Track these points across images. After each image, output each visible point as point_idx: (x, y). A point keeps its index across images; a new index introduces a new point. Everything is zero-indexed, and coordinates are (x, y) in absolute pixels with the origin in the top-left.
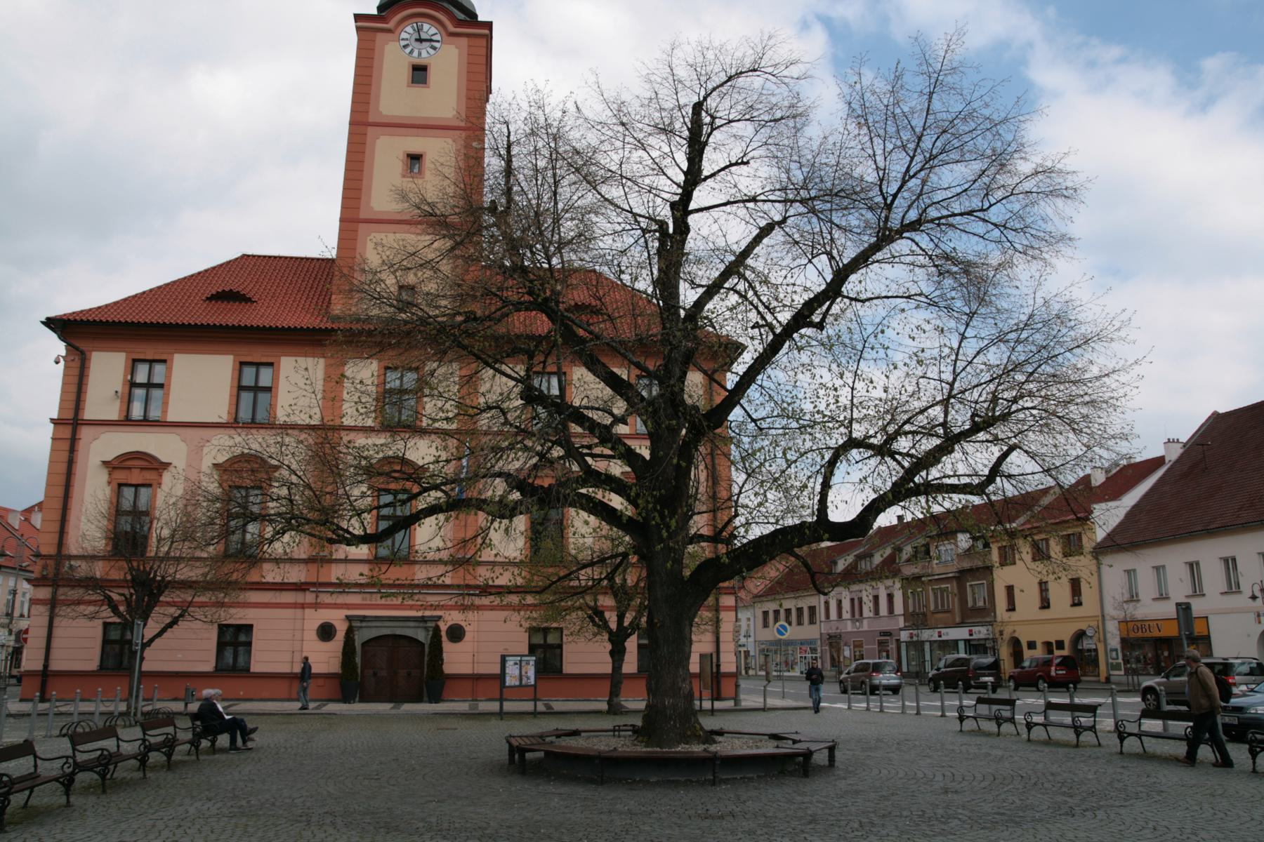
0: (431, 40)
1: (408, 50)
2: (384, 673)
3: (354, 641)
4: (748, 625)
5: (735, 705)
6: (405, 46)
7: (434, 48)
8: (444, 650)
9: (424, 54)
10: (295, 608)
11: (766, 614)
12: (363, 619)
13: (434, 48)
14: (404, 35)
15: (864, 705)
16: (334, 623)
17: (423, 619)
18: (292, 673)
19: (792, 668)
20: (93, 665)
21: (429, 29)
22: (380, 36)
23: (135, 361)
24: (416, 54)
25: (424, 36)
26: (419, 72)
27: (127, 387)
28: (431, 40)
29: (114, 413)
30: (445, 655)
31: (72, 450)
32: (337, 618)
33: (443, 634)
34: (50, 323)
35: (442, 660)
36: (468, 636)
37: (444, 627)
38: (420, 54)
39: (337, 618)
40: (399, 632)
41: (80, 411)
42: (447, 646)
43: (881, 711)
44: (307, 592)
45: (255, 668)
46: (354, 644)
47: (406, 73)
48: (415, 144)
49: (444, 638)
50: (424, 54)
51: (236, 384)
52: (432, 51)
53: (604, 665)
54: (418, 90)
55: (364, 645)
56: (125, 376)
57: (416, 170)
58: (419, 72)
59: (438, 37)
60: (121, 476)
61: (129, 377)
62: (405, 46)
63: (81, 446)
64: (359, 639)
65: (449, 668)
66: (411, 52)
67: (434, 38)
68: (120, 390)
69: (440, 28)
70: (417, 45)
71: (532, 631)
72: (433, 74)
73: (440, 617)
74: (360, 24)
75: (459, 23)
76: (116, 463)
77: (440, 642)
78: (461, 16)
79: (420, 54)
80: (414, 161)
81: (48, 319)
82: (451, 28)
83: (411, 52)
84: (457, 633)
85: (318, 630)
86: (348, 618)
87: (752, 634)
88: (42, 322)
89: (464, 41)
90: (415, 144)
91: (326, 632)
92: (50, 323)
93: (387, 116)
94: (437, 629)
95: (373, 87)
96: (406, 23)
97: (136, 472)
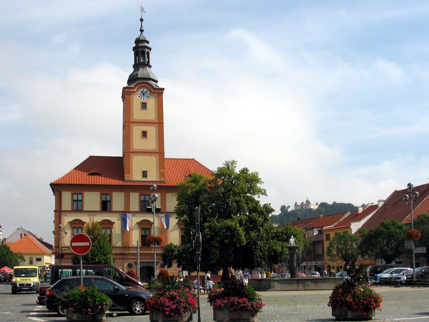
6: (139, 97)
13: (148, 97)
16: (131, 263)
23: (73, 194)
26: (144, 106)
29: (70, 209)
38: (144, 99)
44: (124, 255)
47: (140, 106)
52: (147, 98)
54: (144, 111)
58: (144, 106)
60: (74, 226)
62: (139, 97)
66: (141, 98)
69: (150, 91)
79: (144, 99)
82: (153, 91)
93: (135, 119)
95: (131, 110)
96: (140, 88)
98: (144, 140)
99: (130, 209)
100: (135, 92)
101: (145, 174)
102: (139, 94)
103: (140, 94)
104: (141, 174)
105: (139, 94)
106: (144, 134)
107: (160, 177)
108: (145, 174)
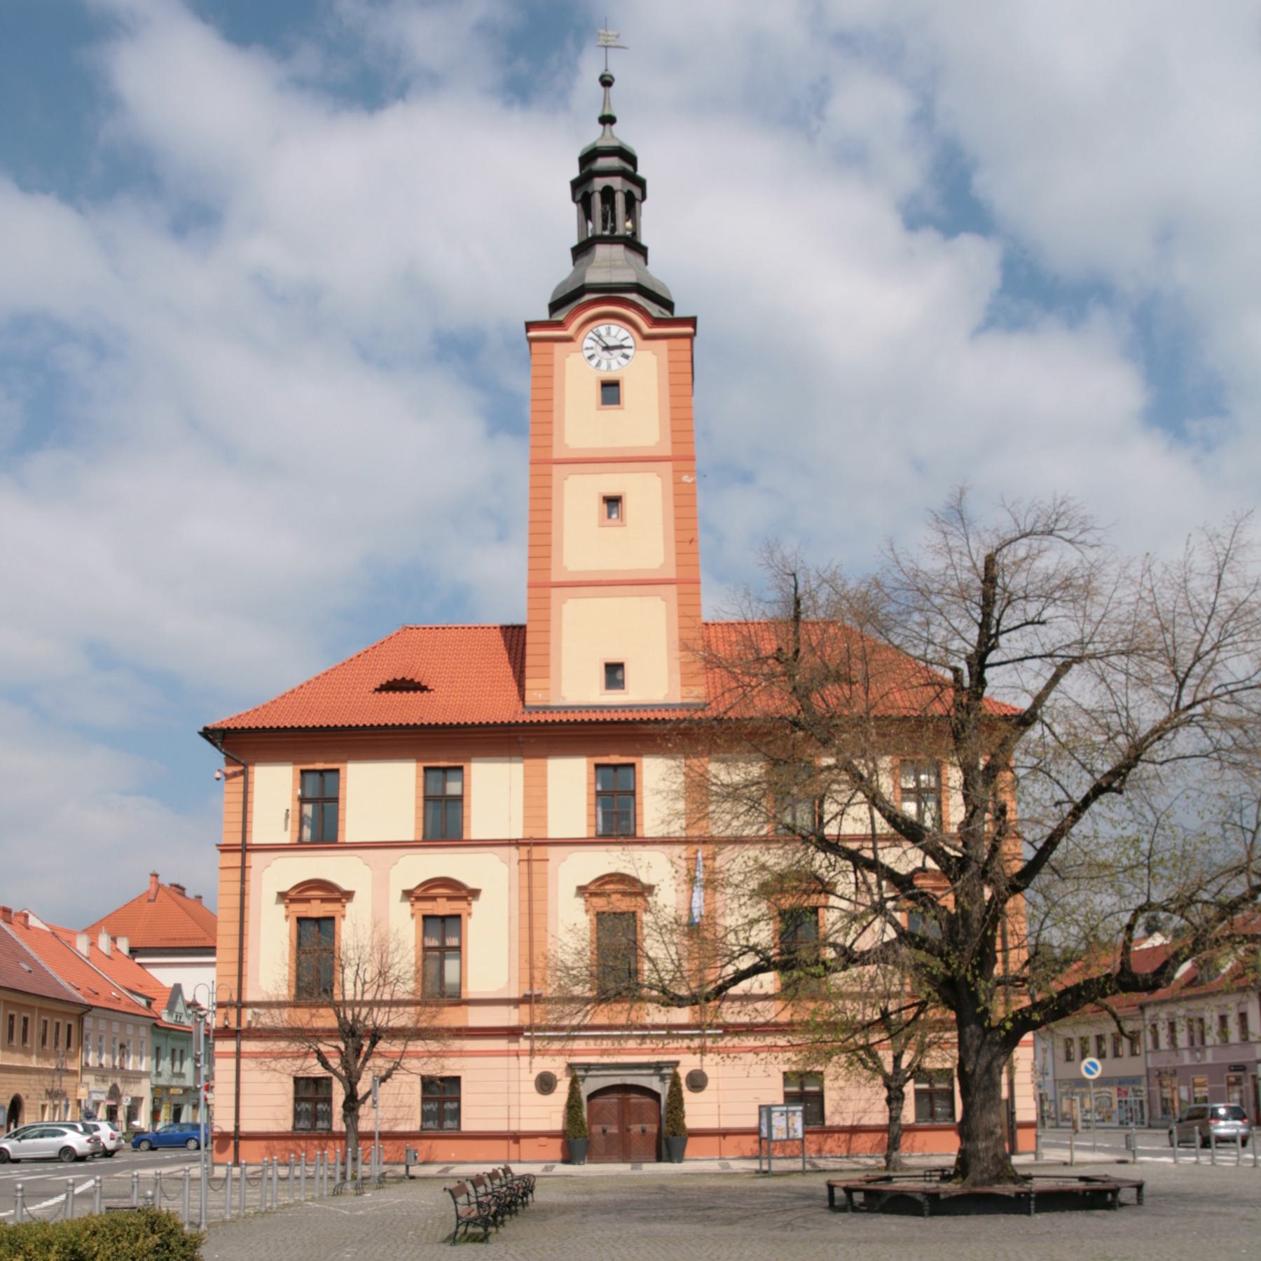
0: (622, 347)
1: (594, 362)
2: (613, 1130)
3: (579, 1093)
4: (1044, 1058)
5: (1036, 1159)
6: (590, 357)
7: (626, 357)
8: (686, 1100)
9: (613, 366)
10: (508, 1056)
11: (1068, 1043)
12: (588, 1067)
13: (626, 357)
14: (588, 343)
15: (1194, 1159)
17: (658, 1067)
18: (508, 1132)
19: (1109, 1117)
20: (286, 1125)
21: (616, 332)
22: (558, 347)
24: (604, 366)
25: (611, 342)
26: (610, 390)
27: (297, 804)
28: (622, 347)
30: (686, 1107)
31: (243, 881)
32: (556, 1065)
33: (683, 1082)
34: (208, 734)
35: (683, 1112)
36: (711, 1084)
37: (683, 1072)
38: (609, 366)
39: (556, 1065)
40: (630, 1081)
41: (248, 835)
42: (687, 1095)
43: (1213, 1164)
45: (467, 1125)
46: (579, 1097)
47: (595, 392)
48: (612, 483)
49: (684, 1088)
50: (614, 365)
51: (421, 794)
52: (623, 361)
53: (878, 1116)
54: (611, 412)
55: (591, 1097)
56: (294, 790)
57: (614, 516)
58: (610, 390)
59: (629, 342)
61: (299, 792)
62: (590, 357)
63: (252, 875)
64: (587, 1088)
65: (691, 1122)
66: (598, 364)
67: (625, 343)
68: (289, 807)
70: (606, 354)
71: (787, 1077)
72: (626, 391)
73: (677, 1063)
74: (533, 334)
75: (657, 322)
76: (293, 894)
77: (680, 1092)
78: (655, 310)
79: (609, 366)
80: (611, 504)
81: (206, 729)
82: (646, 329)
83: (598, 364)
84: (698, 1082)
85: (536, 1082)
86: (571, 1067)
87: (1050, 1070)
88: (200, 733)
89: (663, 344)
90: (612, 483)
91: (546, 1084)
92: (208, 734)
94: (675, 1077)
95: (556, 414)
97: (316, 903)
98: (613, 532)
99: (545, 827)
100: (569, 340)
101: (614, 673)
102: (587, 349)
103: (592, 348)
104: (600, 675)
105: (587, 349)
106: (613, 502)
107: (683, 685)
108: (614, 673)
